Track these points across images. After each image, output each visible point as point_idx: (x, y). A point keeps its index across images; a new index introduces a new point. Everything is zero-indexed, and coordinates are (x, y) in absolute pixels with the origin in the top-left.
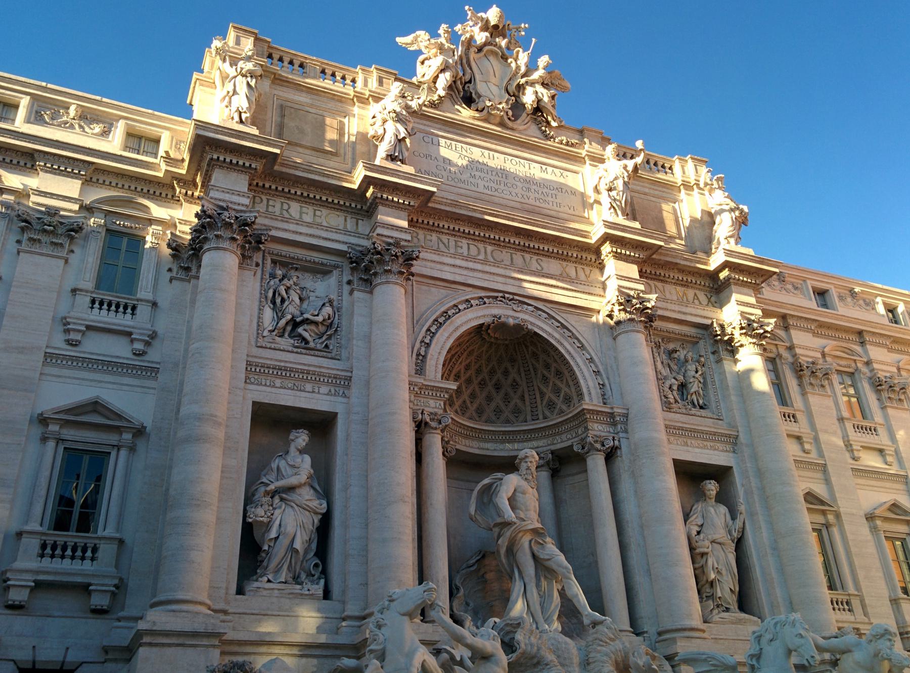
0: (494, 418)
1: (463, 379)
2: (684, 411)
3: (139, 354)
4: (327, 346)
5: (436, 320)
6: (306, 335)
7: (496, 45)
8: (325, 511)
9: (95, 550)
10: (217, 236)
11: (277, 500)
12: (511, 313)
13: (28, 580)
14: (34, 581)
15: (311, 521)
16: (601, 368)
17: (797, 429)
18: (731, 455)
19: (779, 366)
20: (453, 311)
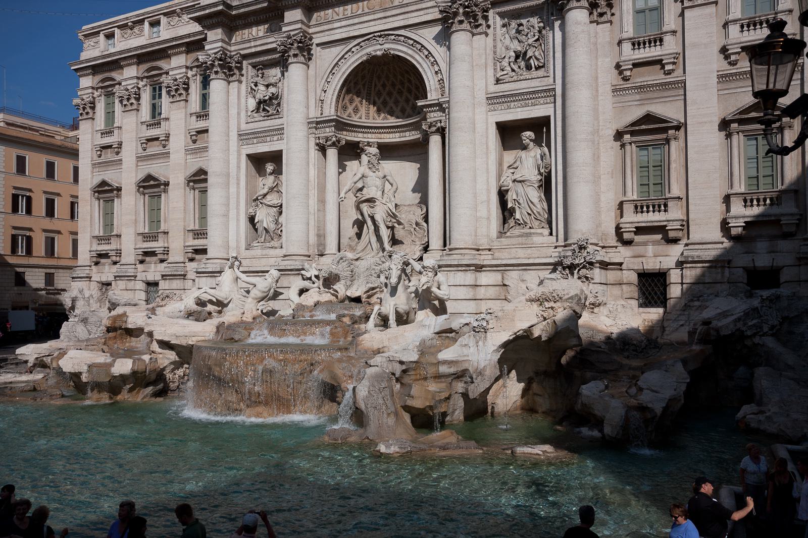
2: (515, 78)
5: (331, 72)
12: (379, 47)
20: (342, 61)
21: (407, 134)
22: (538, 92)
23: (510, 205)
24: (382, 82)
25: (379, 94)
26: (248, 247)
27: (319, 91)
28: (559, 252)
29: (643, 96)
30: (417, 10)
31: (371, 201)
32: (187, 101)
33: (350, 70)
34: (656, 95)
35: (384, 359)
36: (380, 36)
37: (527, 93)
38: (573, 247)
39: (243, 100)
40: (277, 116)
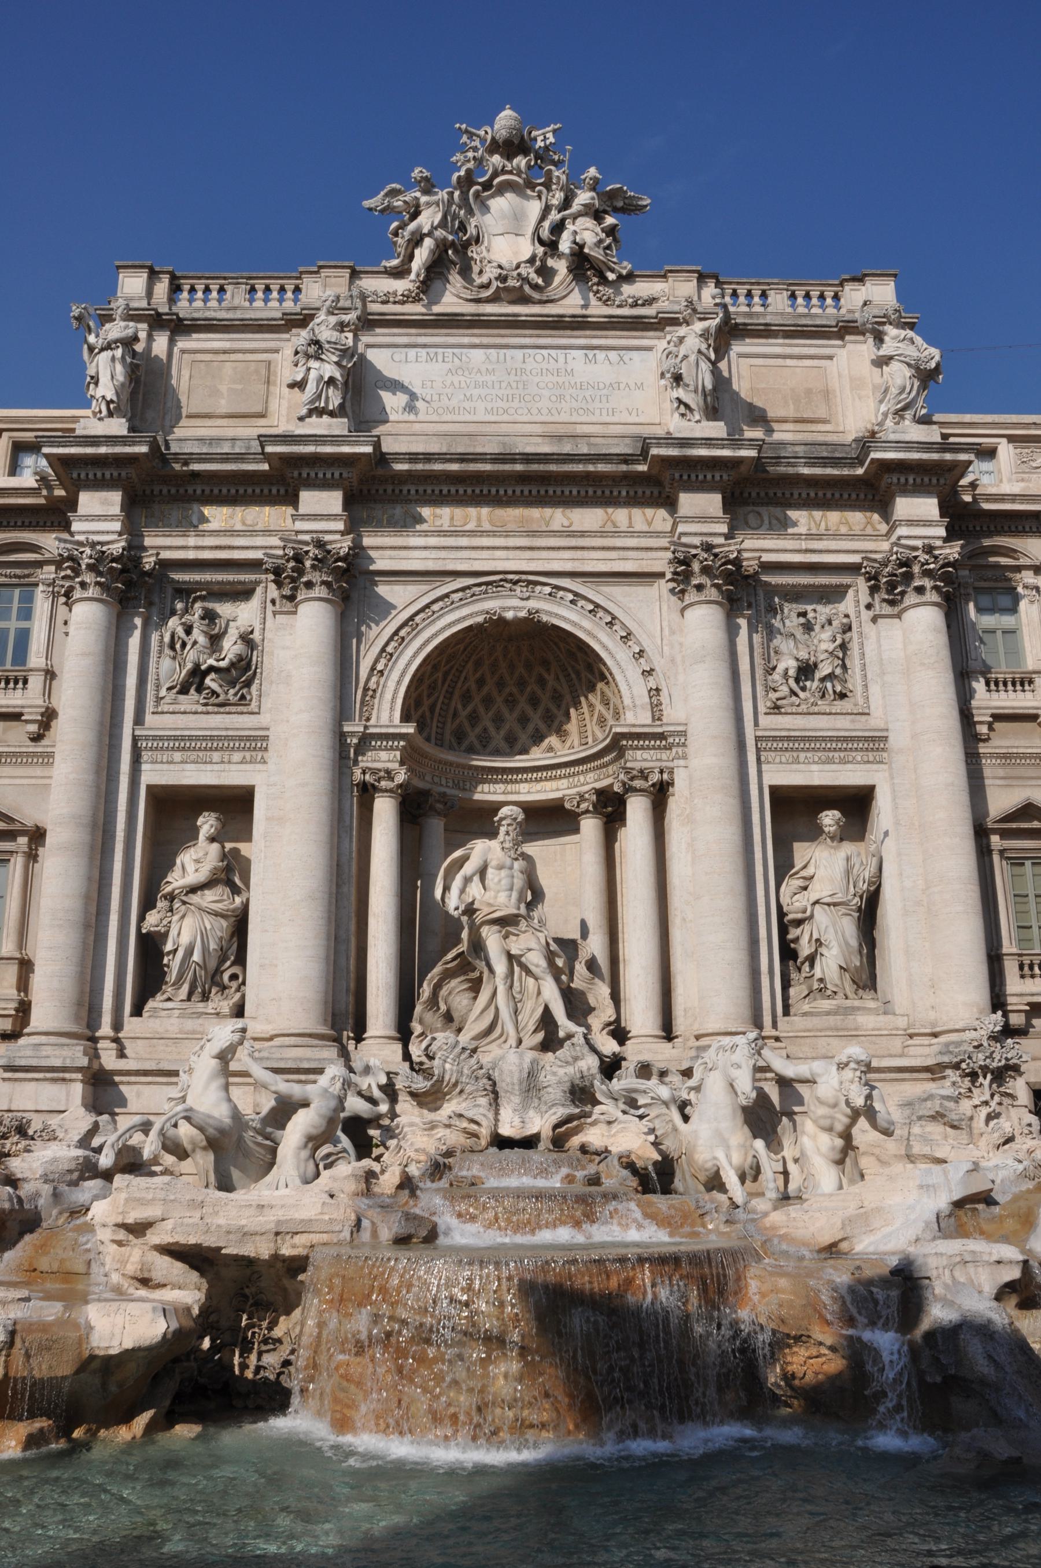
1: (477, 700)
2: (803, 708)
3: (37, 738)
4: (243, 697)
5: (396, 633)
6: (214, 686)
7: (510, 172)
11: (177, 904)
12: (515, 602)
15: (220, 928)
16: (659, 663)
18: (875, 767)
20: (422, 615)
21: (524, 787)
22: (852, 739)
24: (478, 675)
25: (466, 698)
28: (947, 1045)
30: (603, 548)
34: (1031, 772)
35: (944, 1261)
36: (516, 583)
37: (831, 739)
38: (970, 1035)
40: (240, 709)
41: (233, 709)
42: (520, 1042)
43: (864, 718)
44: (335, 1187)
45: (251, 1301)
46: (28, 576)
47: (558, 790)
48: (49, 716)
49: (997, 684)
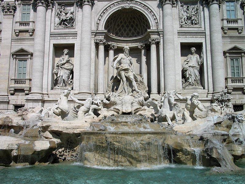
0: (132, 36)
1: (120, 26)
2: (188, 26)
5: (103, 12)
6: (66, 23)
8: (71, 69)
9: (25, 82)
10: (39, 2)
12: (128, 5)
13: (13, 89)
14: (14, 89)
15: (68, 72)
16: (158, 17)
17: (237, 26)
19: (236, 4)
20: (109, 8)
21: (130, 44)
22: (198, 33)
23: (187, 76)
25: (118, 26)
26: (52, 89)
27: (96, 19)
29: (232, 40)
31: (126, 70)
32: (14, 16)
33: (112, 12)
34: (235, 40)
39: (53, 19)
40: (71, 28)
41: (70, 28)
42: (128, 94)
43: (201, 28)
44: (87, 121)
45: (70, 142)
46: (29, 2)
47: (137, 44)
48: (34, 30)
49: (229, 22)
